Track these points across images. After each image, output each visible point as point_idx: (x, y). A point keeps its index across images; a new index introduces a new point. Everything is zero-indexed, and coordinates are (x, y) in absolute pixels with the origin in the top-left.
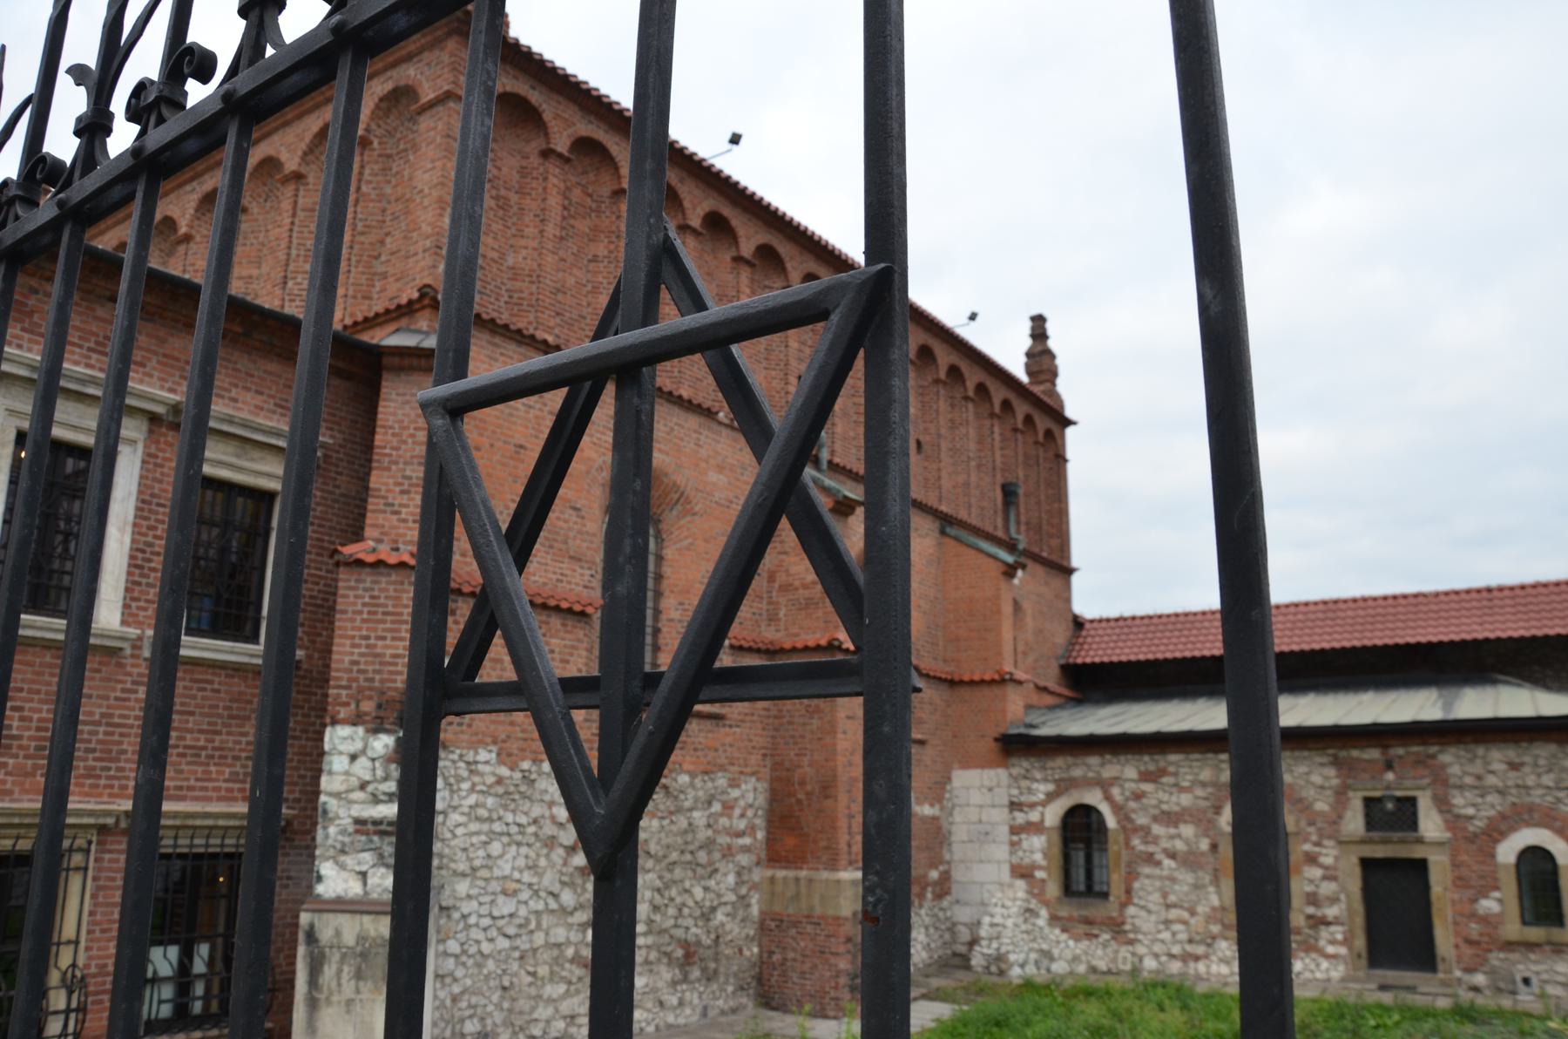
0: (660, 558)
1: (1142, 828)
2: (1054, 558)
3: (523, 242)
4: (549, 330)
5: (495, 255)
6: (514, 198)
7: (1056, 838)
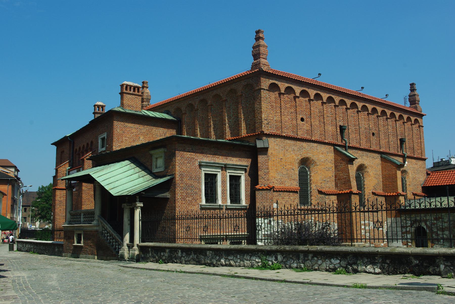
0: (310, 176)
1: (435, 232)
2: (420, 156)
3: (277, 114)
4: (285, 133)
5: (272, 118)
6: (274, 104)
7: (413, 235)
